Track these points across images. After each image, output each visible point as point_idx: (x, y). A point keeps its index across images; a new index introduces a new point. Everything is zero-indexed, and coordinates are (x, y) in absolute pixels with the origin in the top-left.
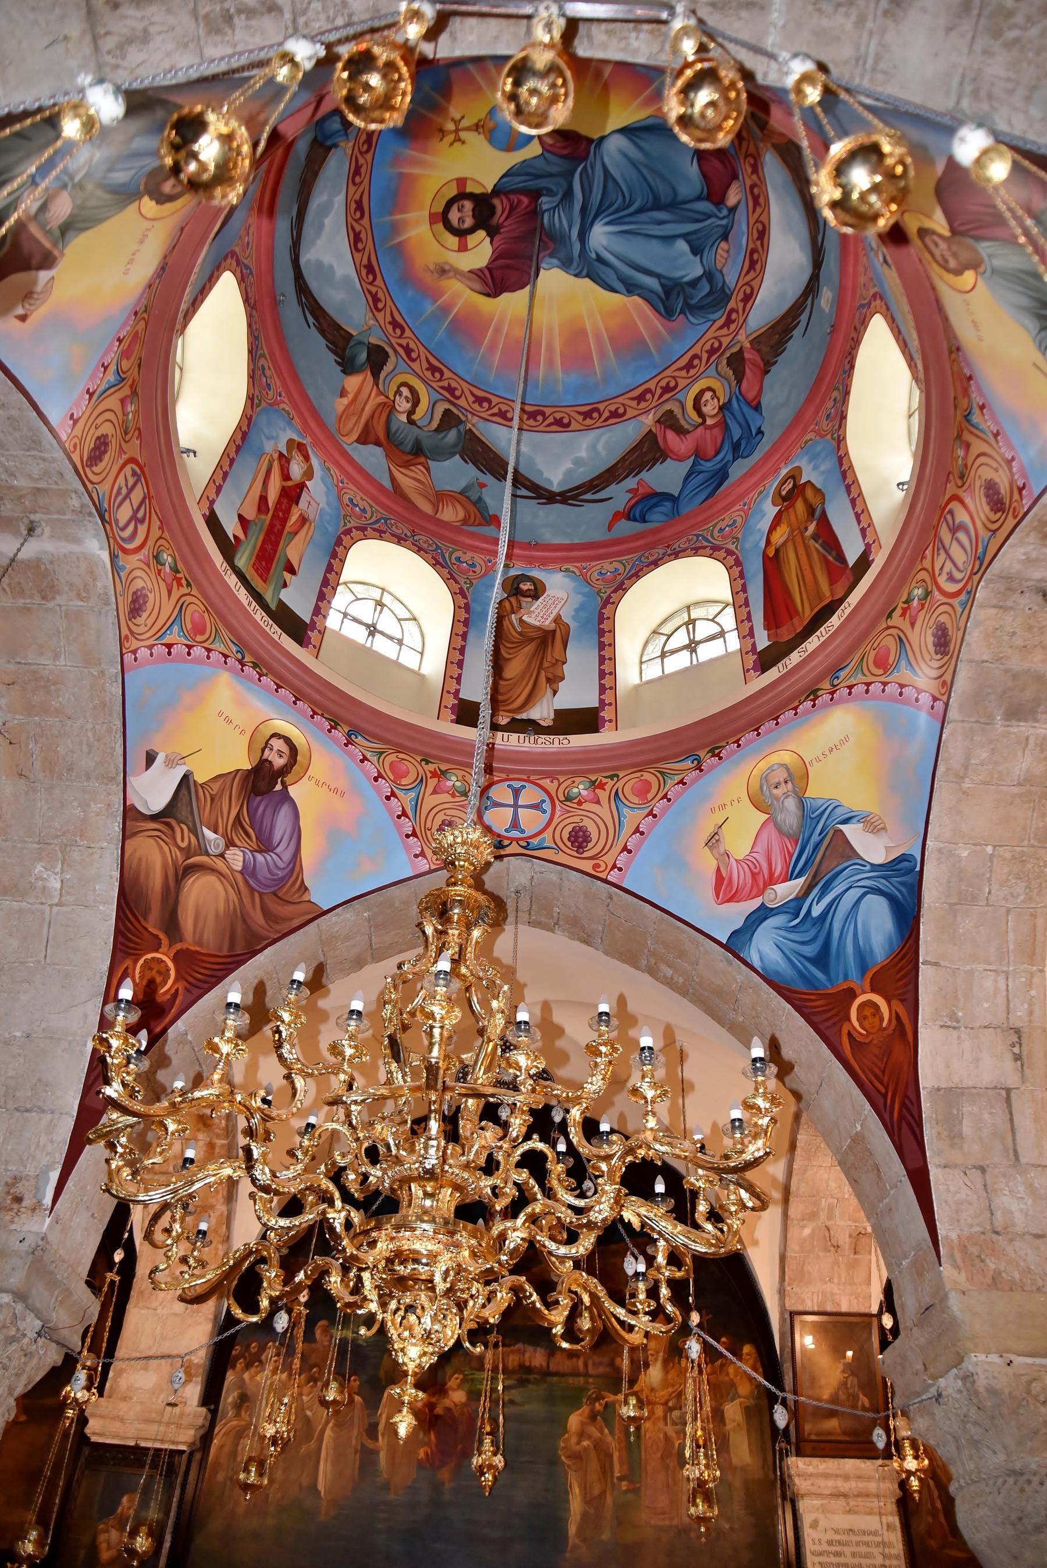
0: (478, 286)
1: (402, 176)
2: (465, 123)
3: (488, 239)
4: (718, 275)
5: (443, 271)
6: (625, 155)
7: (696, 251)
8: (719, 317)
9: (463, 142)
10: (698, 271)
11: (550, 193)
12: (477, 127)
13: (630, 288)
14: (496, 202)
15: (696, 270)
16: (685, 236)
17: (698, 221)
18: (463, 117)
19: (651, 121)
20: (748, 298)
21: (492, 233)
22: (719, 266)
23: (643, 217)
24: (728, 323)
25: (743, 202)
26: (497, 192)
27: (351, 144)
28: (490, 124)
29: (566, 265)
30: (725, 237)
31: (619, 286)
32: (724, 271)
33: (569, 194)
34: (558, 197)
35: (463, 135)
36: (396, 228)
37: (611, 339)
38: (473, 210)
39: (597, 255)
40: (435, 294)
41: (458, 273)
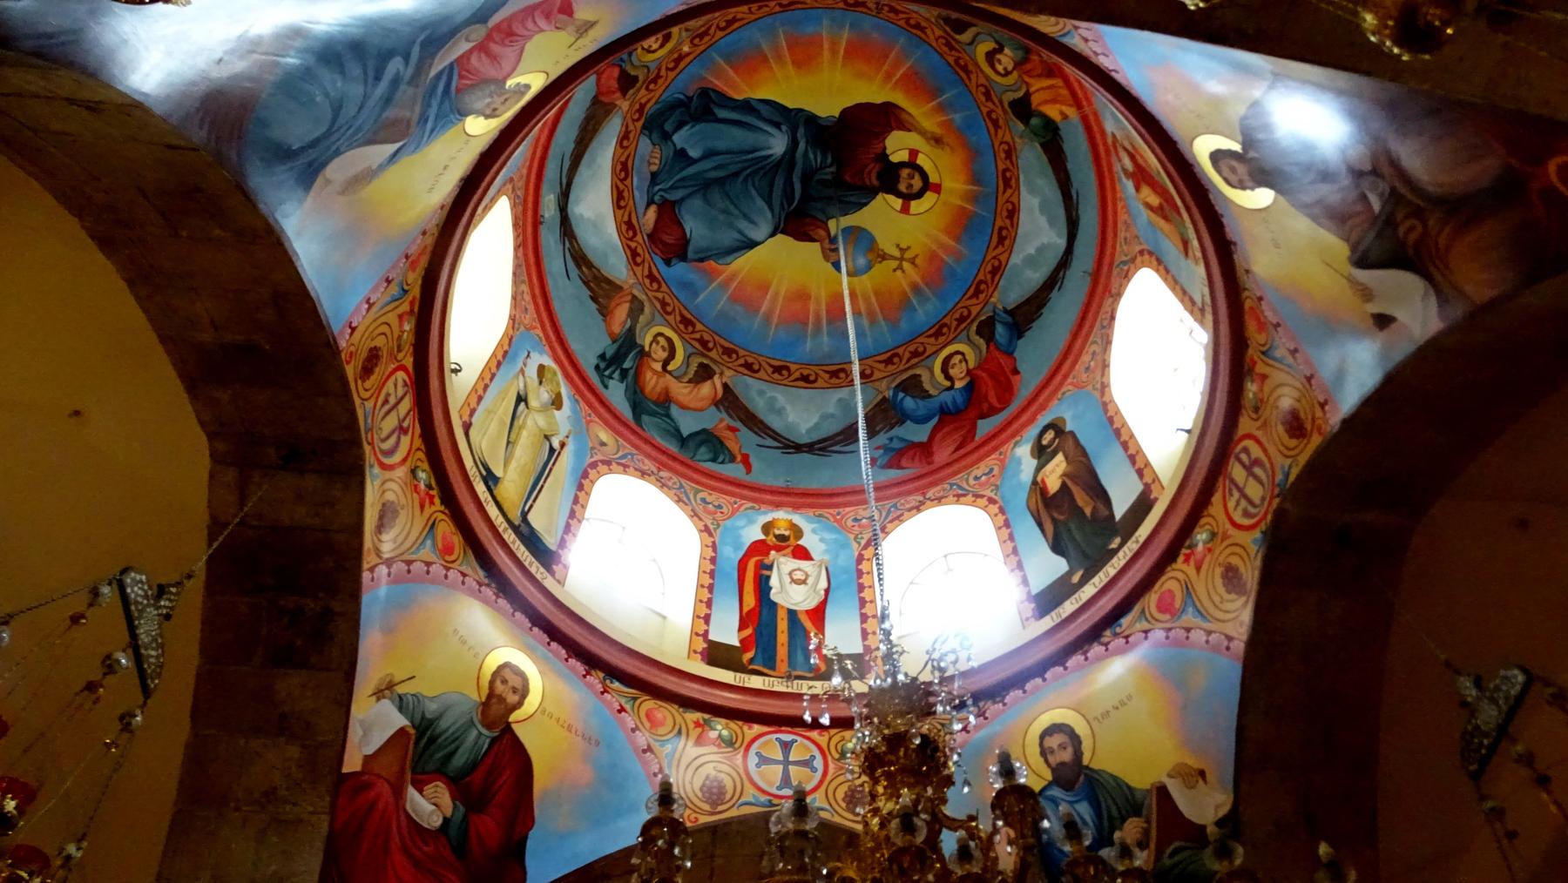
0: (904, 116)
1: (957, 239)
2: (894, 264)
3: (888, 152)
4: (657, 140)
5: (937, 141)
6: (752, 222)
7: (681, 154)
8: (650, 108)
9: (898, 246)
10: (676, 137)
11: (823, 182)
12: (884, 257)
13: (747, 106)
14: (875, 182)
15: (679, 139)
16: (694, 161)
17: (682, 179)
18: (895, 270)
19: (729, 259)
20: (624, 137)
21: (883, 156)
22: (657, 149)
23: (733, 168)
24: (641, 110)
25: (640, 216)
26: (872, 193)
27: (992, 300)
28: (871, 256)
29: (811, 120)
30: (654, 175)
31: (760, 107)
32: (651, 147)
33: (807, 178)
34: (818, 177)
35: (897, 254)
36: (974, 198)
37: (765, 60)
38: (898, 182)
39: (780, 130)
40: (947, 125)
41: (922, 133)
